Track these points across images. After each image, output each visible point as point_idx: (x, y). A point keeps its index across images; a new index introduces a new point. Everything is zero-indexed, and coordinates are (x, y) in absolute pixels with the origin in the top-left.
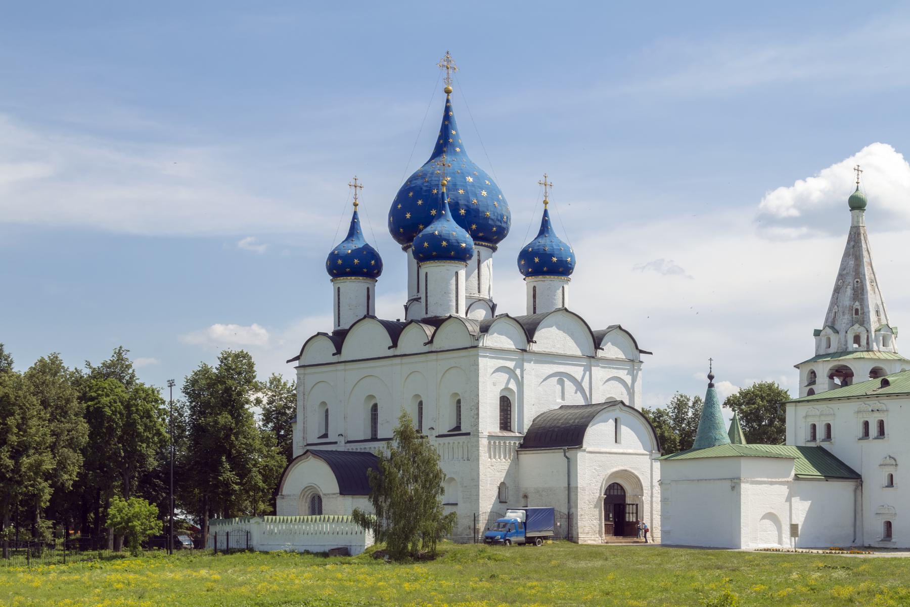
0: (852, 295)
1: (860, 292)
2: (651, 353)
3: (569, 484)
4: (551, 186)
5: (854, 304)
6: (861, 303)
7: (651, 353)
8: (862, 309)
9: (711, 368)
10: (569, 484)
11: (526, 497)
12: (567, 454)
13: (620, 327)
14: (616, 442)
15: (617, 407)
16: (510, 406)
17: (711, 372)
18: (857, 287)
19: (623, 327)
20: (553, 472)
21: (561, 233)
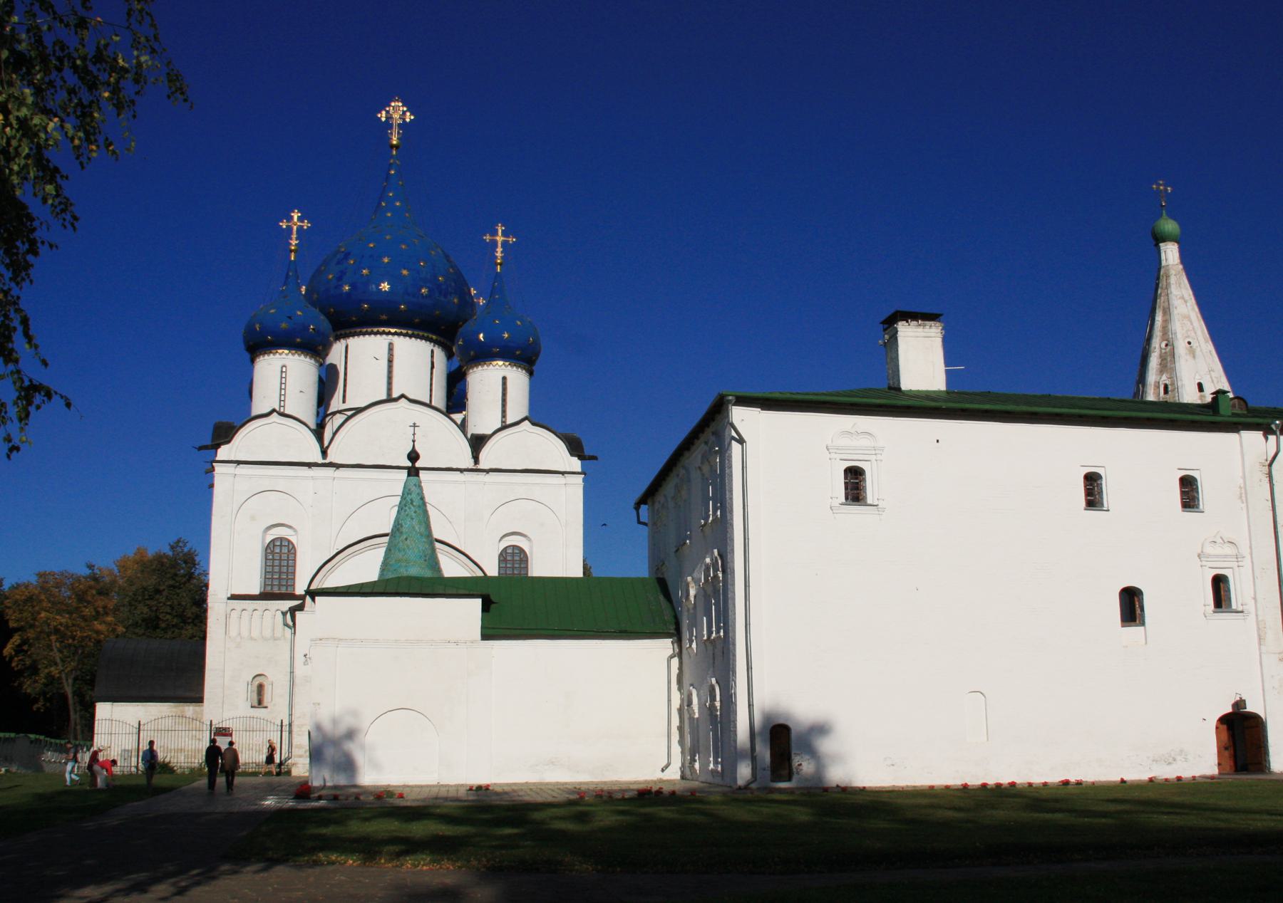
0: (1159, 366)
1: (1169, 359)
5: (1161, 378)
6: (1171, 375)
8: (1172, 384)
9: (414, 441)
18: (1166, 353)
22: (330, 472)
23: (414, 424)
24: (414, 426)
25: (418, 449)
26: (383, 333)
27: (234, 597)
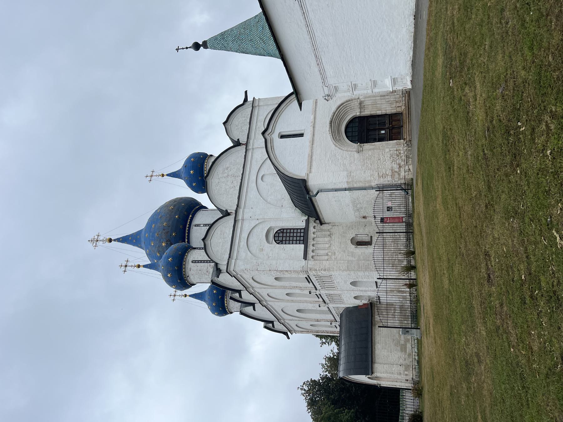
2: (246, 92)
3: (345, 189)
4: (153, 171)
7: (246, 92)
9: (187, 48)
10: (345, 189)
11: (364, 217)
12: (315, 193)
13: (225, 123)
14: (301, 135)
15: (268, 137)
16: (283, 229)
17: (190, 48)
19: (225, 120)
20: (335, 201)
21: (179, 165)
22: (241, 211)
23: (176, 49)
24: (177, 50)
25: (191, 45)
26: (189, 228)
27: (305, 257)
